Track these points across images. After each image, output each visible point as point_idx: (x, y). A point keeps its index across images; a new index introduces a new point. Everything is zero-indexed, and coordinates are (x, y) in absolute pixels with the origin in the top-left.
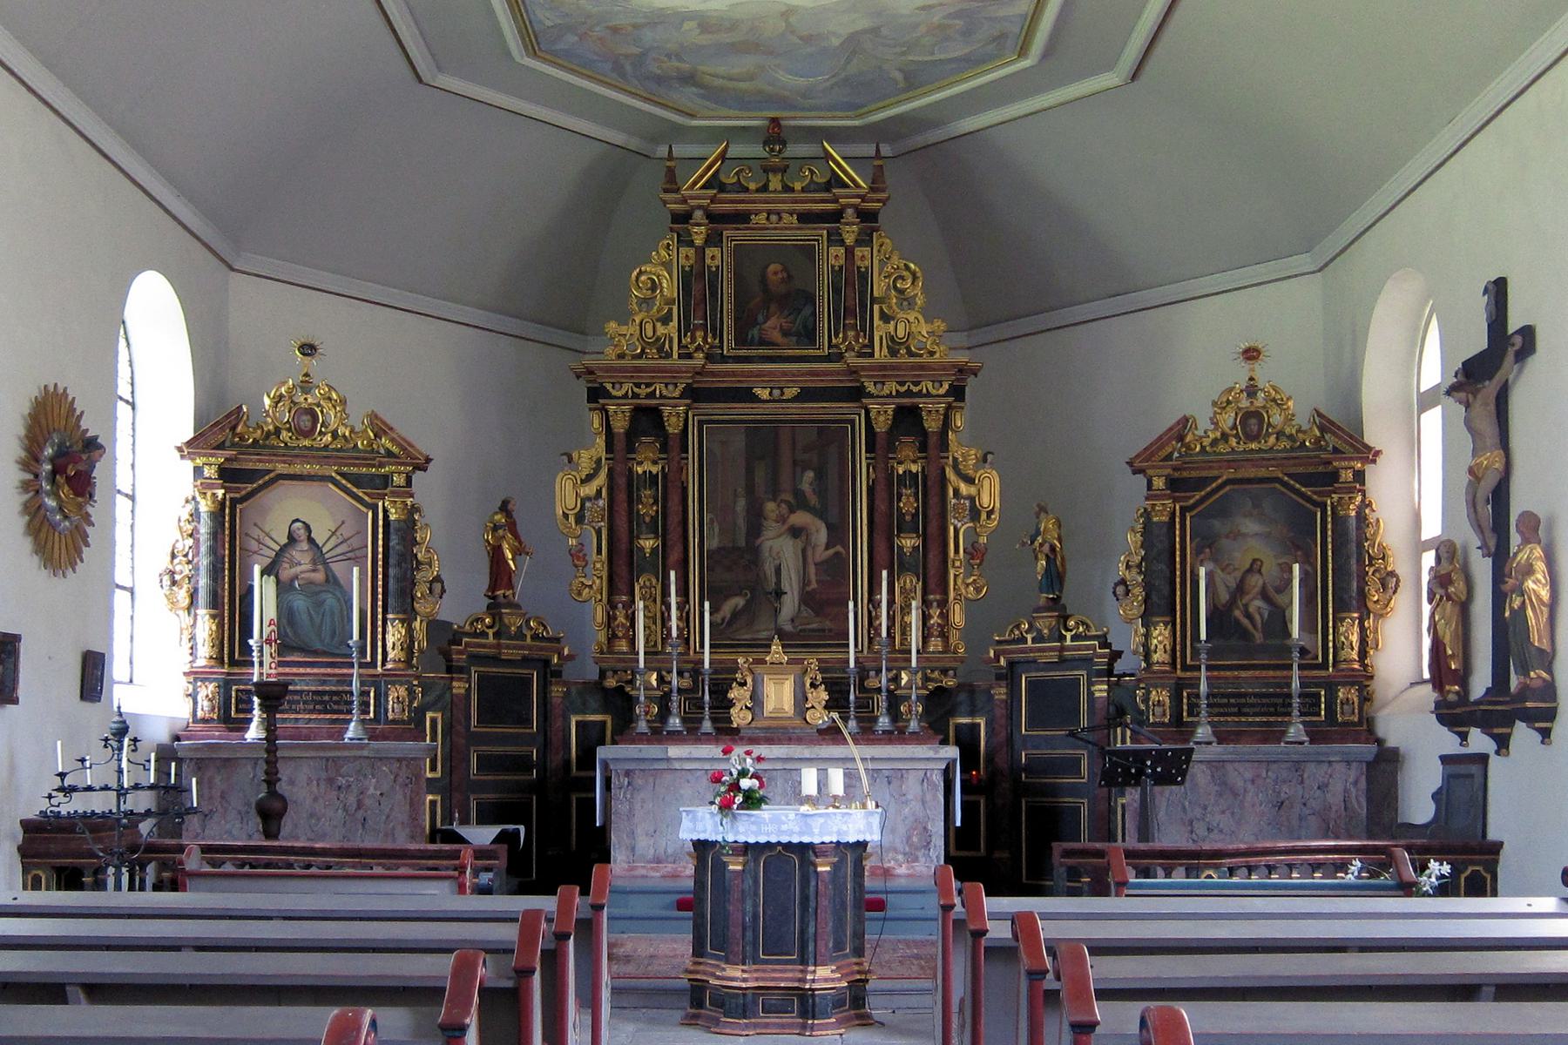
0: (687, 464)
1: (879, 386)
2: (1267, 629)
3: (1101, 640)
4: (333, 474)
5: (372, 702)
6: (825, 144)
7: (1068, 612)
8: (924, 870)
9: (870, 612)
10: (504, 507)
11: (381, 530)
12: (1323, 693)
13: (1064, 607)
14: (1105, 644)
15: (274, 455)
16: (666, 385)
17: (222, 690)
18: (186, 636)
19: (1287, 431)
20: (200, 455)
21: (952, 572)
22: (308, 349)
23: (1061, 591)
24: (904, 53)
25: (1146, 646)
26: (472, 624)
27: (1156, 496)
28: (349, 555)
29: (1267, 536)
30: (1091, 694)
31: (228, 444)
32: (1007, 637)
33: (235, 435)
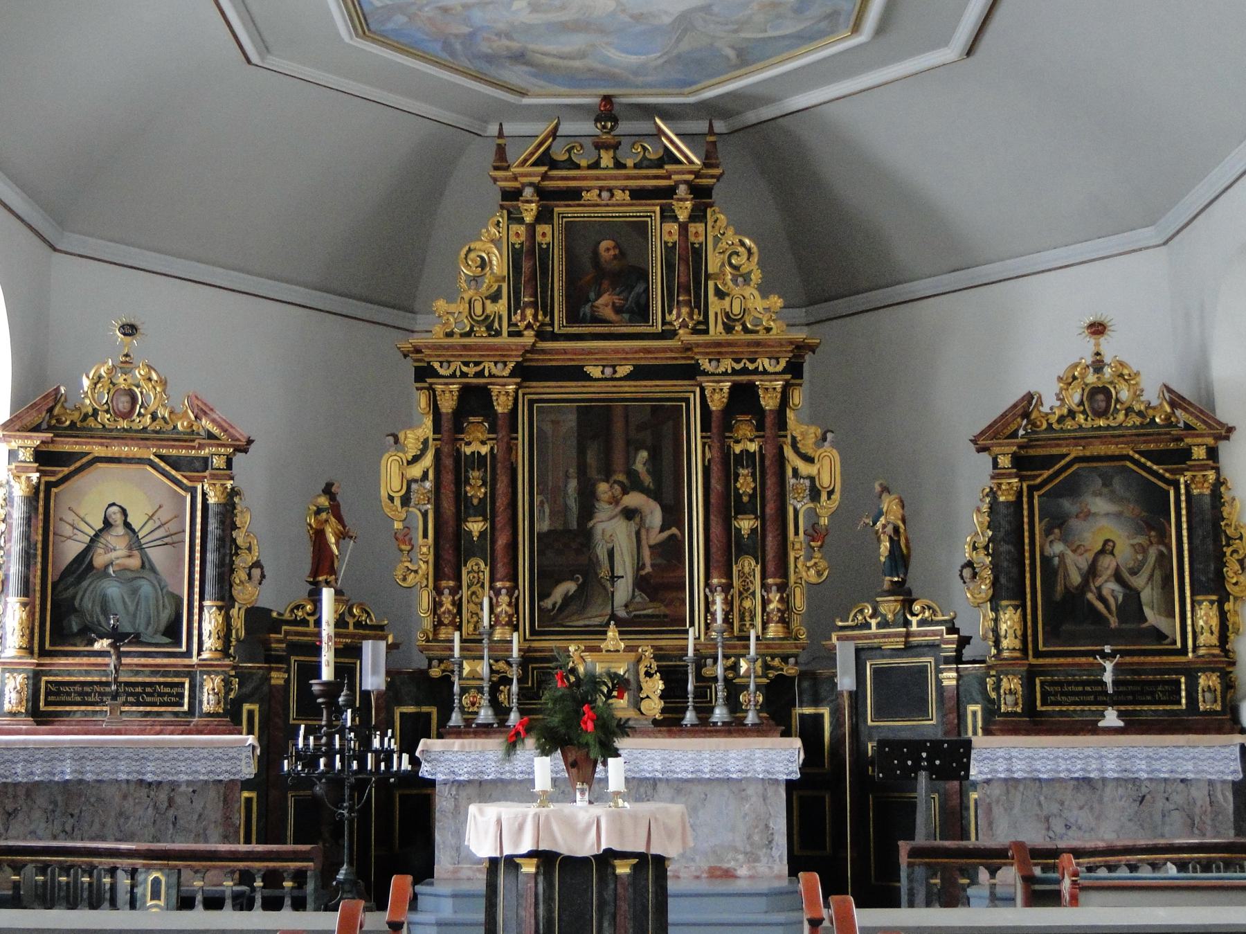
0: (517, 445)
1: (714, 363)
2: (1122, 611)
3: (950, 625)
4: (152, 457)
5: (187, 693)
6: (658, 120)
7: (914, 596)
8: (767, 870)
9: (706, 597)
10: (328, 490)
12: (1183, 680)
13: (909, 592)
14: (952, 630)
15: (92, 437)
16: (496, 363)
17: (31, 682)
19: (1137, 407)
20: (15, 437)
21: (792, 555)
22: (130, 330)
23: (906, 574)
24: (735, 31)
25: (995, 631)
26: (292, 611)
27: (1003, 474)
28: (166, 540)
29: (1119, 515)
30: (939, 682)
31: (44, 426)
32: (850, 623)
33: (51, 417)
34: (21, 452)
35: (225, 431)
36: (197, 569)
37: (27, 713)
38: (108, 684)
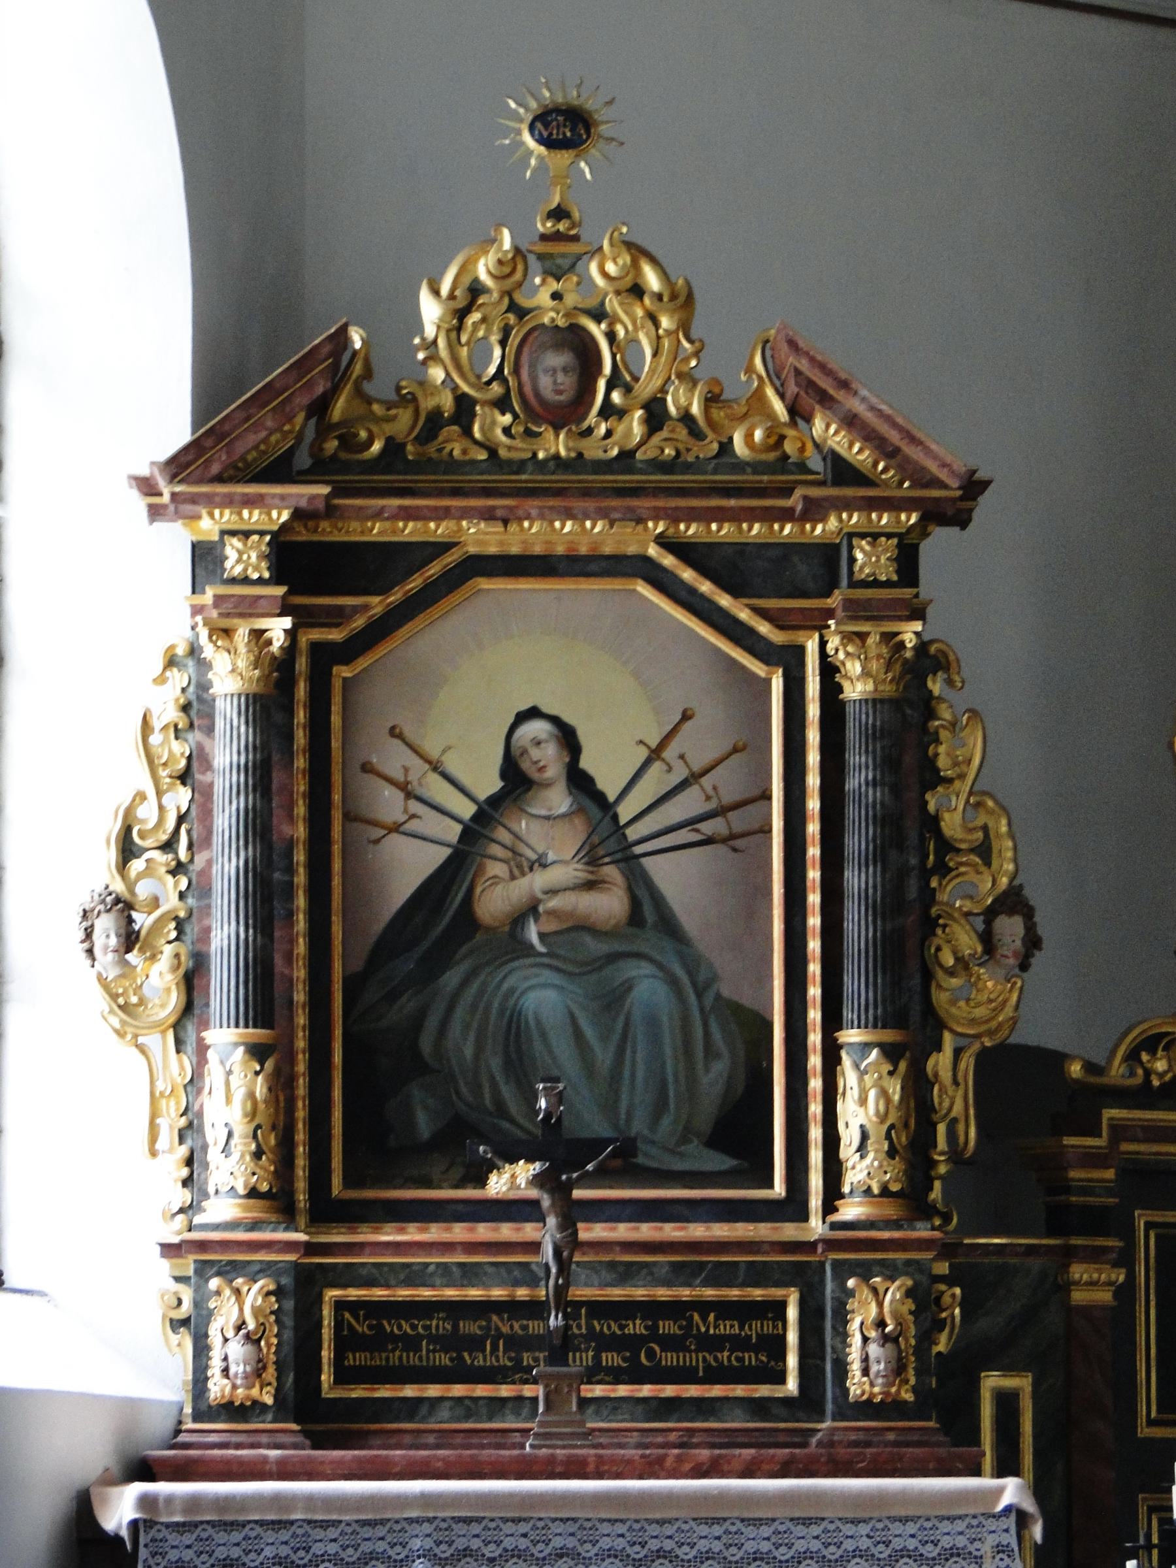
4: (653, 551)
5: (792, 1337)
11: (813, 736)
15: (456, 492)
17: (289, 1304)
18: (170, 1122)
20: (210, 501)
26: (1133, 1056)
28: (707, 827)
31: (303, 460)
33: (324, 429)
34: (232, 549)
35: (887, 451)
36: (814, 921)
37: (281, 1409)
38: (535, 1309)
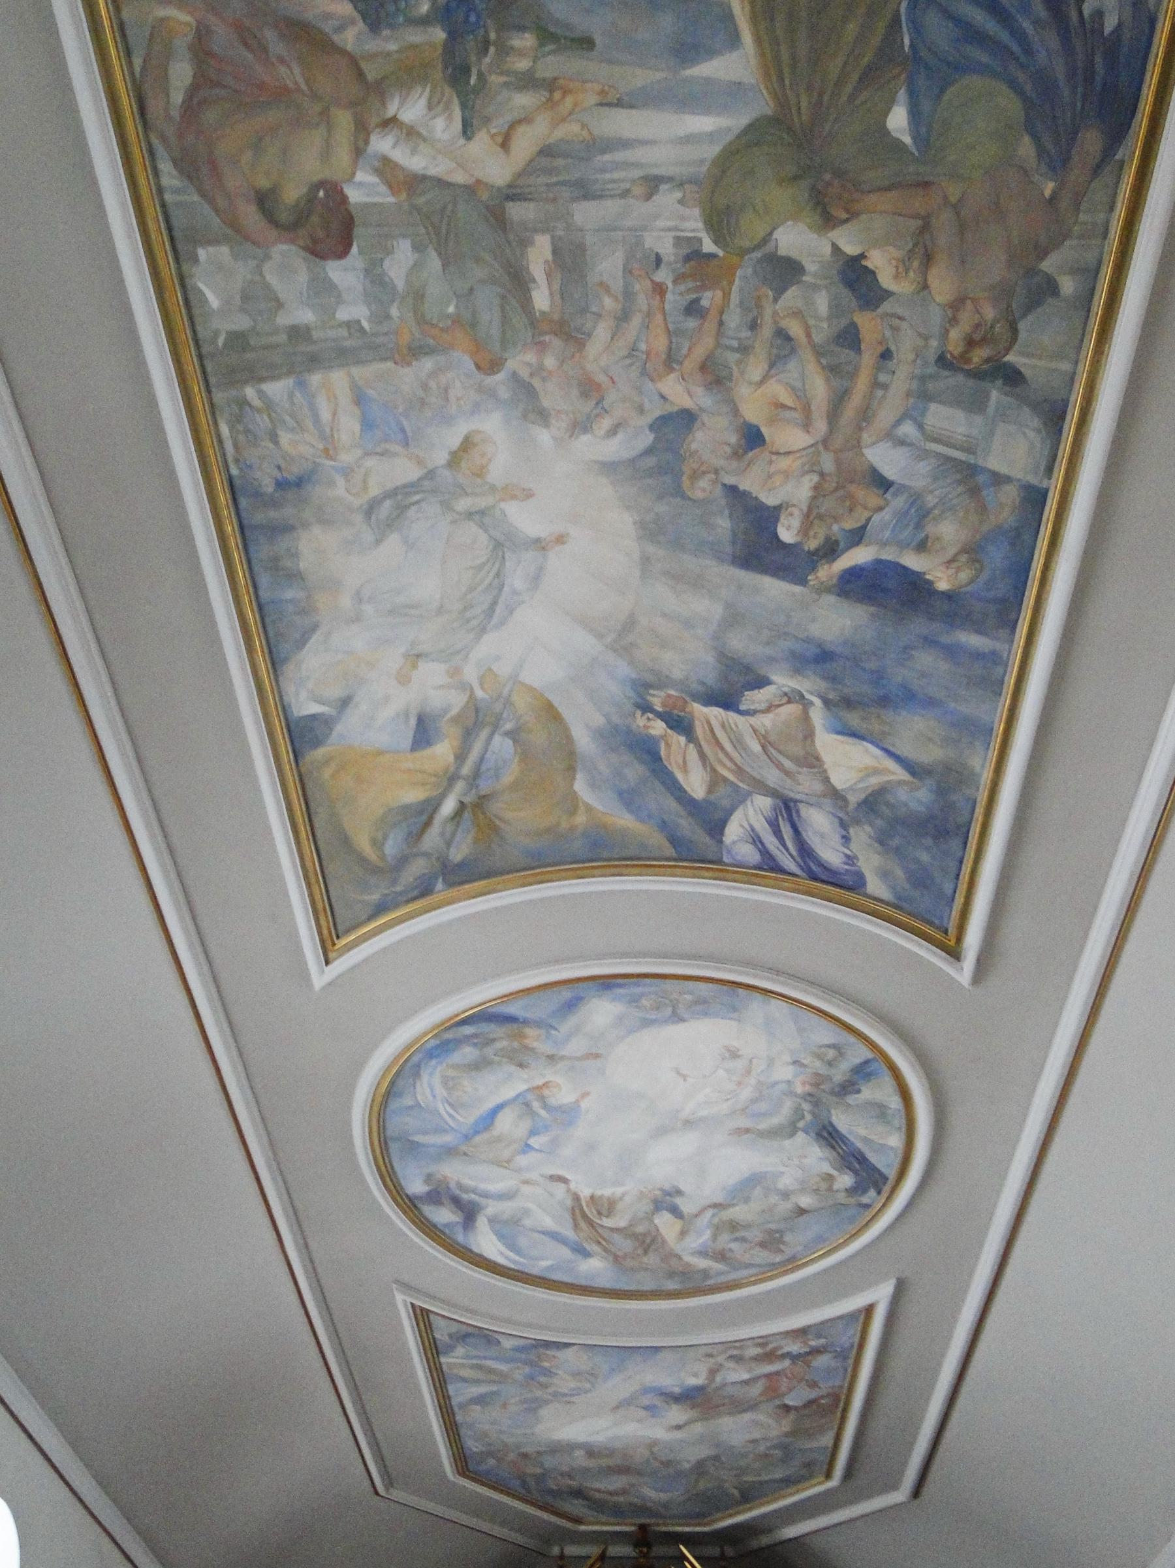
6: (682, 1547)
